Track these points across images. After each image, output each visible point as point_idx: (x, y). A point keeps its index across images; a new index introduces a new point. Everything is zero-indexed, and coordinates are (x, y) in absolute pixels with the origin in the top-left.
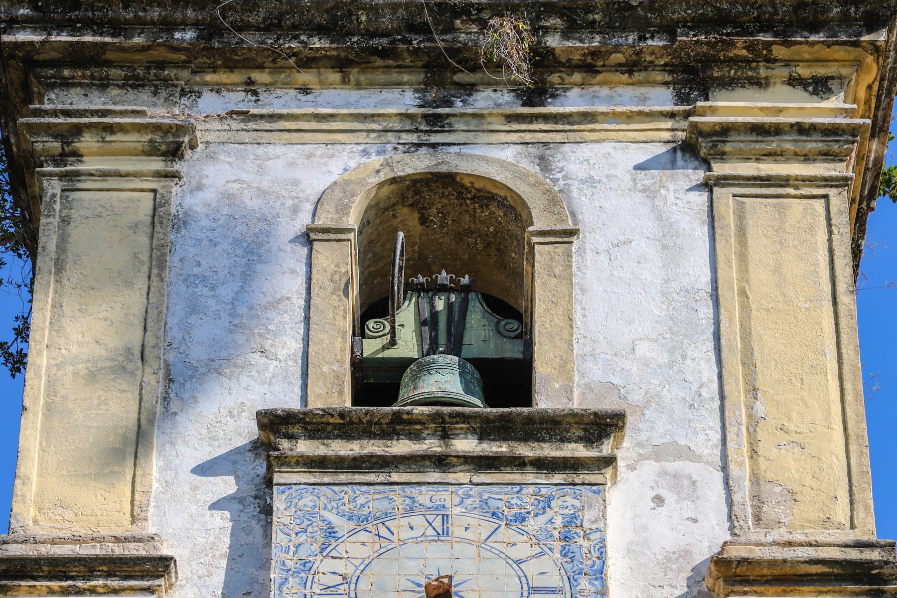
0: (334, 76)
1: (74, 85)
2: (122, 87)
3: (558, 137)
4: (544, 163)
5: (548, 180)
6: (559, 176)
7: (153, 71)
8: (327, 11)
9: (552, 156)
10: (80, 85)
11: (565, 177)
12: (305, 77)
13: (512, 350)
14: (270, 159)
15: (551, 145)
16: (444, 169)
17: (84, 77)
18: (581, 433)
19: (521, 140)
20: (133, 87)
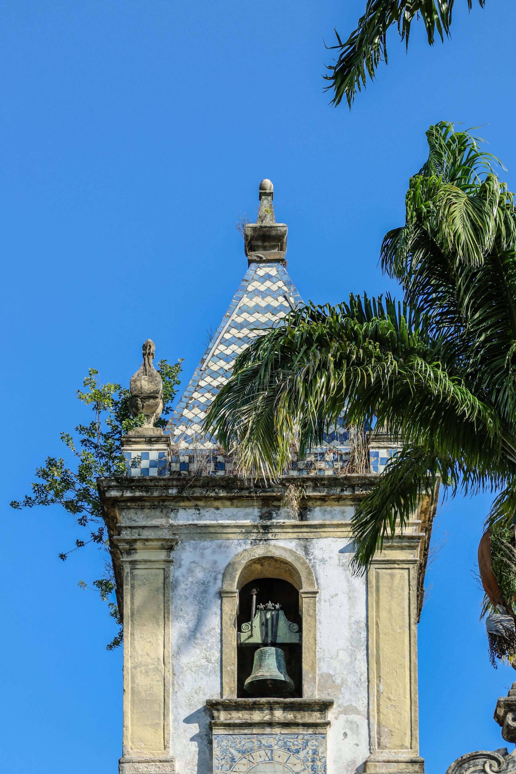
0: (228, 503)
1: (131, 508)
2: (149, 509)
3: (311, 535)
4: (306, 550)
5: (307, 560)
6: (311, 557)
7: (161, 503)
8: (225, 481)
9: (309, 546)
10: (134, 508)
11: (314, 558)
12: (217, 503)
13: (294, 640)
14: (205, 549)
15: (309, 540)
16: (269, 555)
17: (135, 505)
18: (318, 708)
19: (298, 537)
20: (154, 508)
